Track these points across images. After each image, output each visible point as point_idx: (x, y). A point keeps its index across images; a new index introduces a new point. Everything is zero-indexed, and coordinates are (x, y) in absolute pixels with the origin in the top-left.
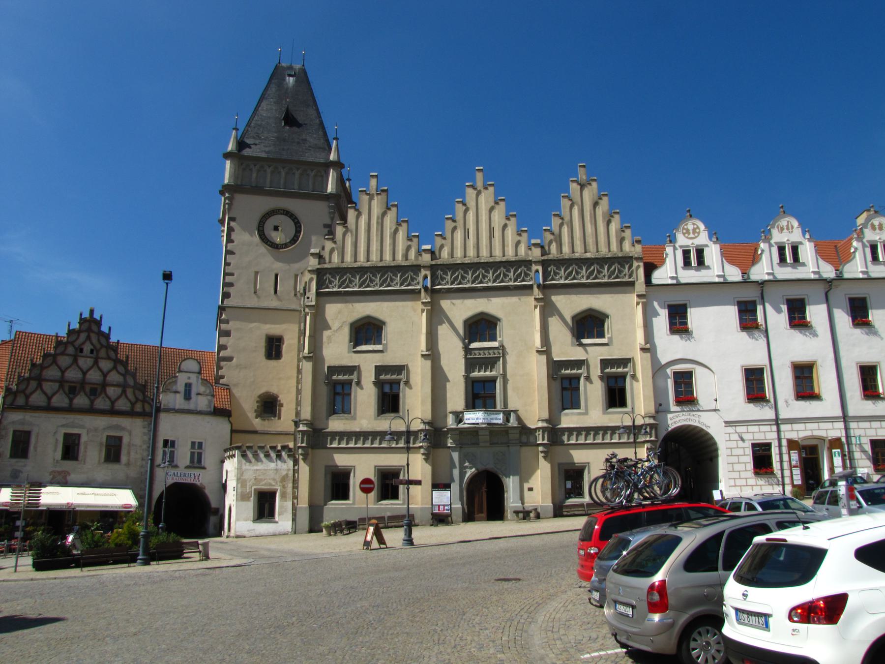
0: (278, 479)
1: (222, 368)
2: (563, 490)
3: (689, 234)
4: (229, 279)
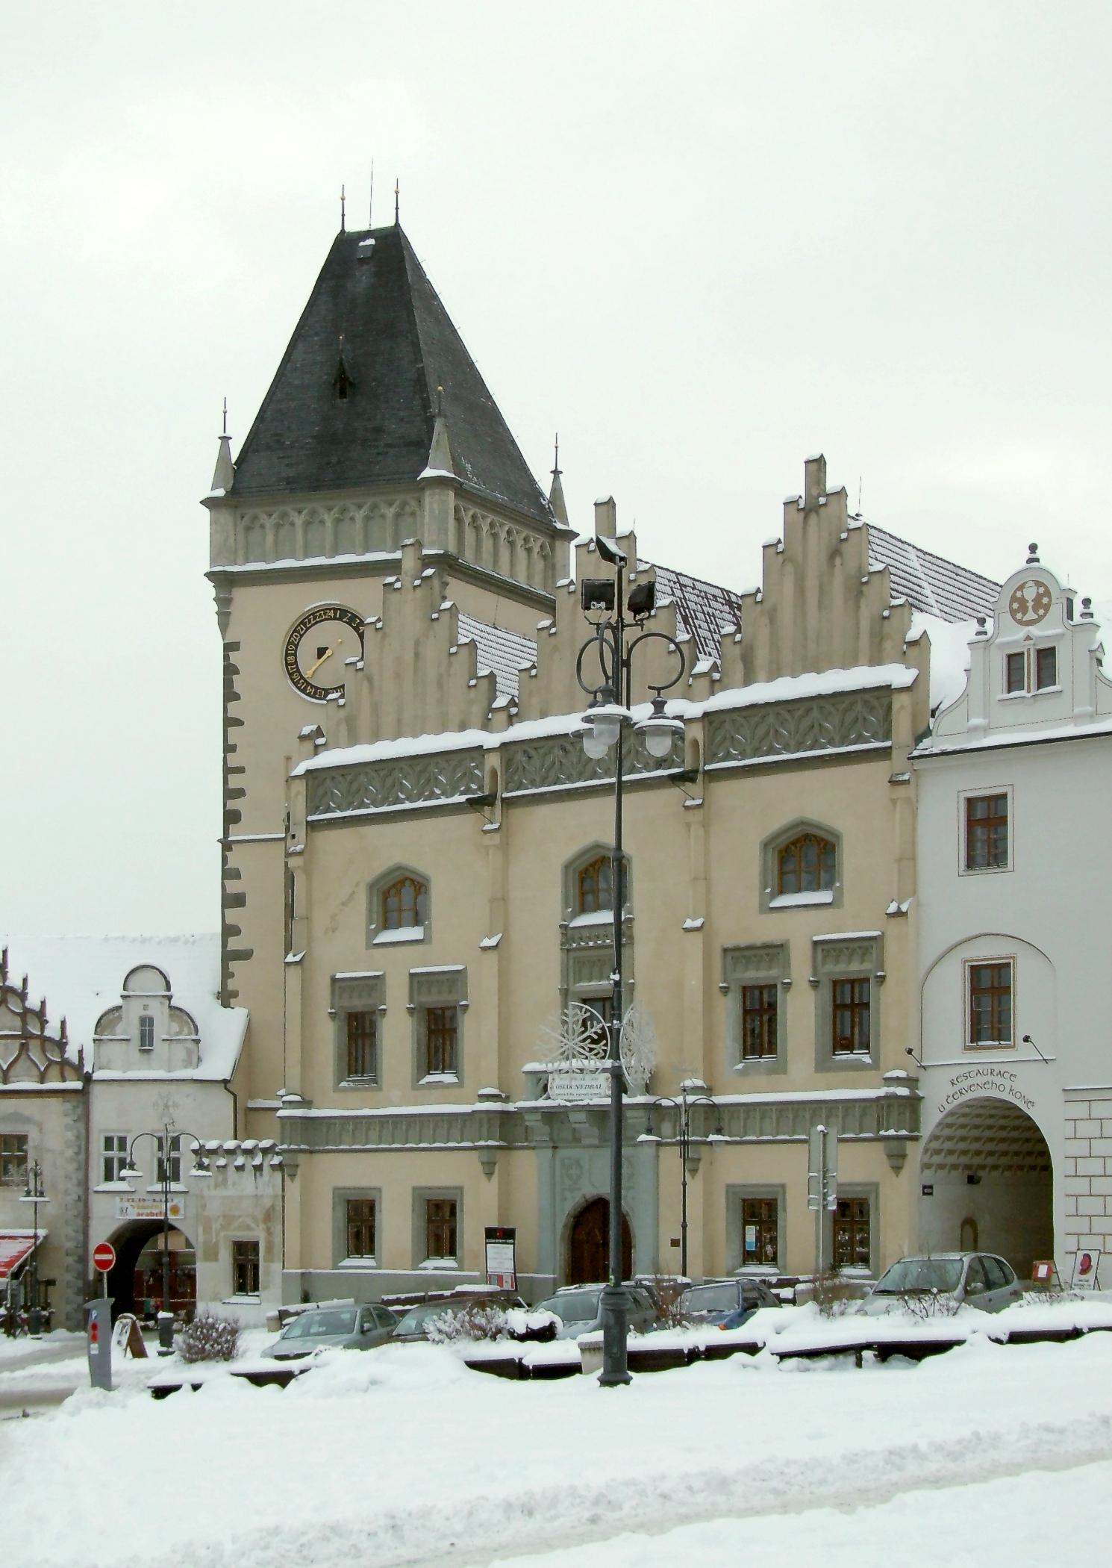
0: (260, 1216)
1: (232, 975)
2: (736, 1247)
3: (1025, 611)
4: (235, 781)
